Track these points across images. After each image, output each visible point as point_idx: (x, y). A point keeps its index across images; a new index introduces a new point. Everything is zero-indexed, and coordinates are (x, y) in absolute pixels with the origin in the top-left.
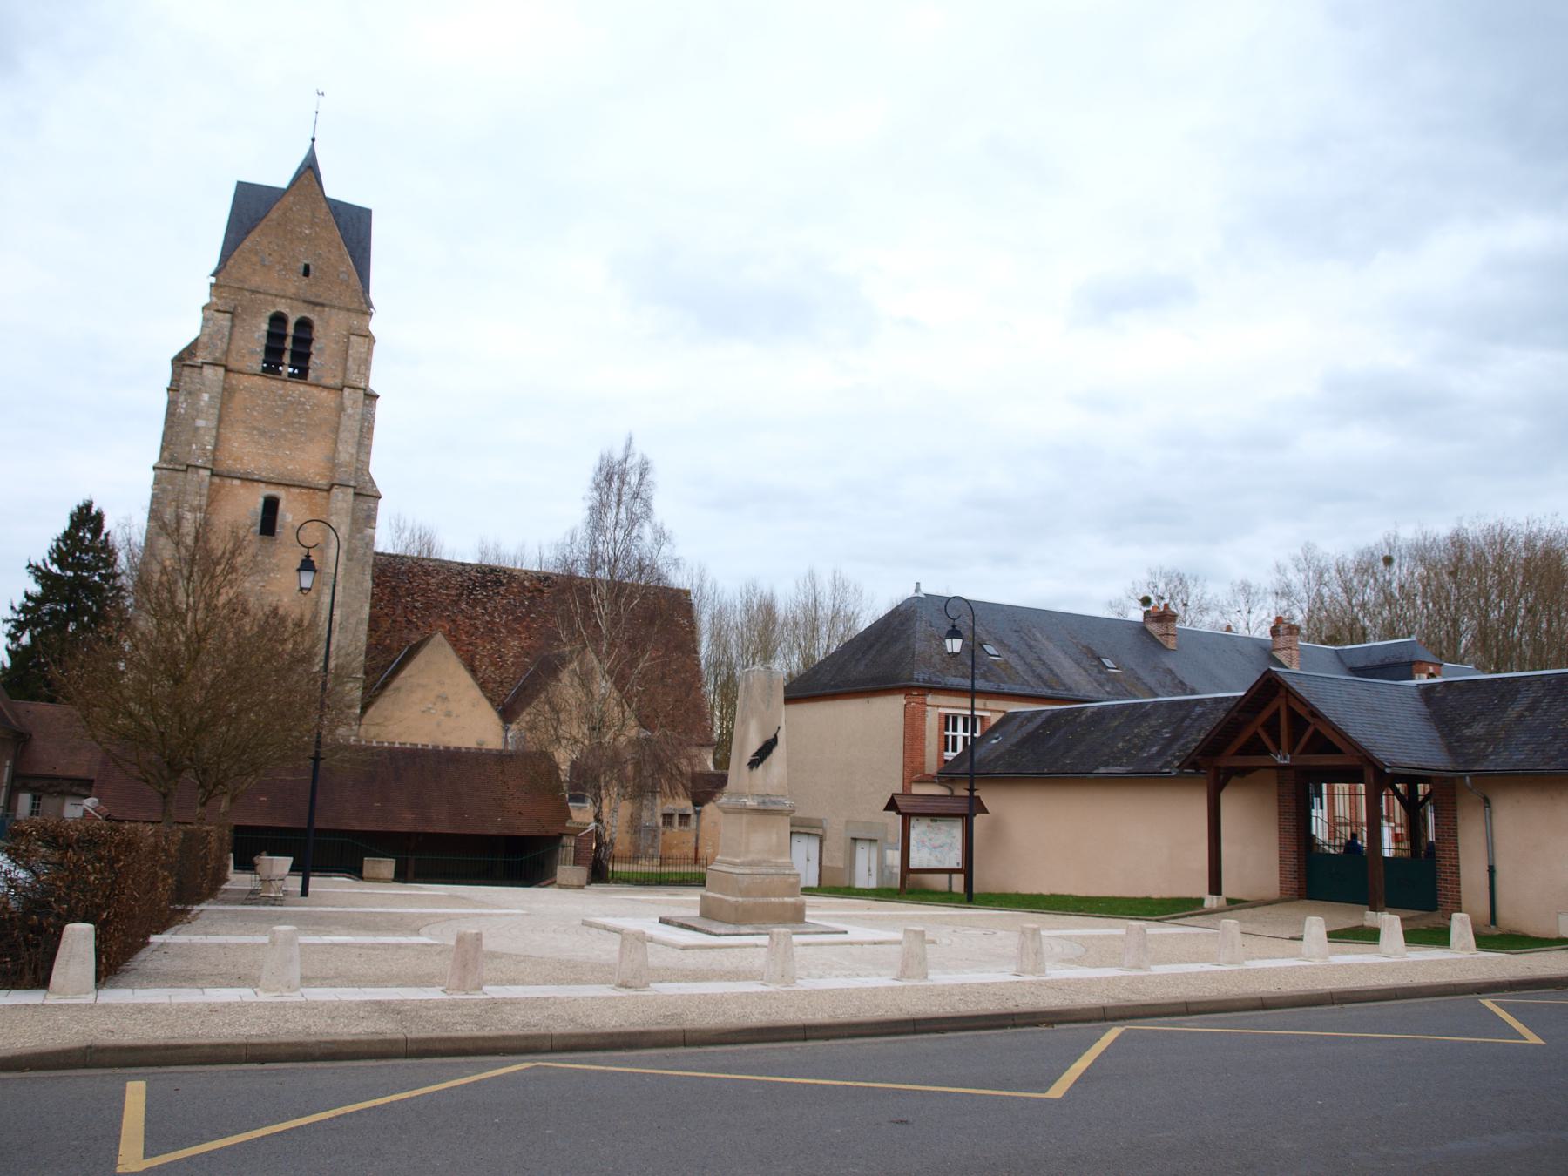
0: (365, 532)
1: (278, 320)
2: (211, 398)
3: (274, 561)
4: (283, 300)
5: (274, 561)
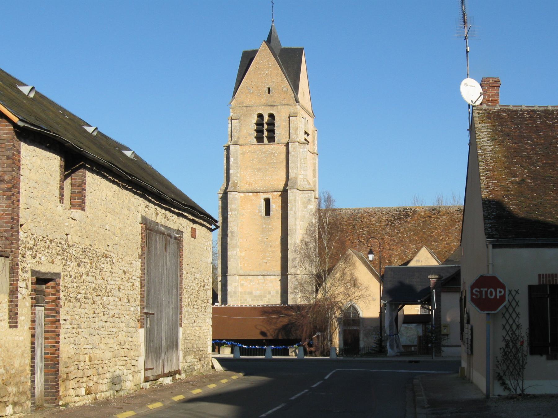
0: (308, 207)
1: (260, 116)
2: (234, 159)
3: (270, 227)
4: (260, 108)
5: (270, 227)
